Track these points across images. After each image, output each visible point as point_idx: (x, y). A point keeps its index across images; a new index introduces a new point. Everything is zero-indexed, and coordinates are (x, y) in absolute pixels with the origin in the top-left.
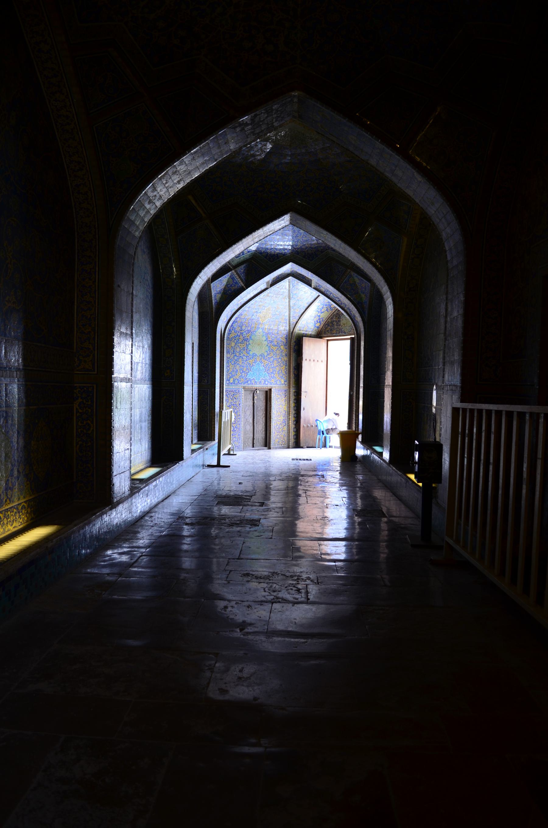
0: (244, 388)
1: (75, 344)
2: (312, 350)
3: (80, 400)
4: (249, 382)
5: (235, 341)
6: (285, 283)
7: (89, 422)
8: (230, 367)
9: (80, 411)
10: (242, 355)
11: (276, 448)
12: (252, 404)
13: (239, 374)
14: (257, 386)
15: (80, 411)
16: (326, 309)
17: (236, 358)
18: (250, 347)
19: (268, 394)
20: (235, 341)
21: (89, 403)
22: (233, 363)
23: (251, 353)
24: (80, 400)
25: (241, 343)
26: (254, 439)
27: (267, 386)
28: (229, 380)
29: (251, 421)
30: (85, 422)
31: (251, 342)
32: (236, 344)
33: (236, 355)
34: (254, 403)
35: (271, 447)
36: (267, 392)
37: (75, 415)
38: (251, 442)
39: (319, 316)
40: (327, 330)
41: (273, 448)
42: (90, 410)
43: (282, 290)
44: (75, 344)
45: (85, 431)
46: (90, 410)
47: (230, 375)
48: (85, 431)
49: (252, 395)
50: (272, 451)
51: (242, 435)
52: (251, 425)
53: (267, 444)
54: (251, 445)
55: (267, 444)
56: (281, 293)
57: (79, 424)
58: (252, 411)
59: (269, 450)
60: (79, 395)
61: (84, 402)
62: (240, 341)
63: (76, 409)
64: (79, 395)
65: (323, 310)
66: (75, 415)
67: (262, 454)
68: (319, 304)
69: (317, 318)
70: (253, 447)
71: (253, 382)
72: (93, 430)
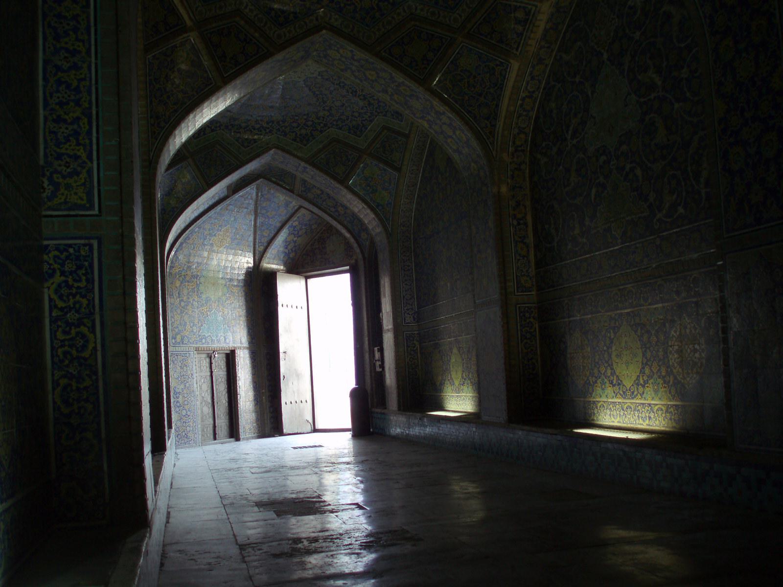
0: (197, 349)
1: (42, 147)
2: (289, 291)
3: (58, 279)
4: (204, 341)
5: (181, 279)
6: (250, 191)
7: (84, 329)
8: (176, 317)
9: (61, 304)
10: (191, 300)
11: (248, 439)
12: (209, 374)
13: (188, 327)
14: (216, 345)
15: (61, 304)
16: (304, 231)
17: (183, 304)
18: (201, 288)
19: (230, 358)
20: (181, 279)
21: (83, 284)
22: (179, 311)
23: (204, 296)
24: (58, 279)
25: (188, 282)
26: (214, 426)
27: (230, 344)
28: (175, 338)
29: (210, 401)
30: (73, 331)
31: (202, 280)
32: (181, 283)
33: (182, 300)
34: (212, 372)
35: (241, 437)
36: (227, 355)
37: (47, 314)
38: (212, 432)
39: (295, 242)
40: (306, 263)
41: (243, 439)
42: (85, 302)
43: (247, 202)
44: (42, 147)
45: (74, 352)
46: (85, 302)
47: (177, 330)
48: (74, 352)
49: (208, 360)
50: (241, 443)
51: (199, 422)
52: (210, 406)
53: (234, 433)
54: (212, 437)
55: (234, 433)
56: (245, 206)
57: (60, 335)
58: (210, 385)
59: (237, 442)
60: (56, 266)
61: (71, 282)
62: (187, 279)
63: (51, 300)
64: (56, 266)
65: (300, 233)
66: (47, 314)
67: (226, 449)
68: (297, 223)
69: (292, 245)
70: (215, 439)
71: (209, 340)
72: (95, 348)
